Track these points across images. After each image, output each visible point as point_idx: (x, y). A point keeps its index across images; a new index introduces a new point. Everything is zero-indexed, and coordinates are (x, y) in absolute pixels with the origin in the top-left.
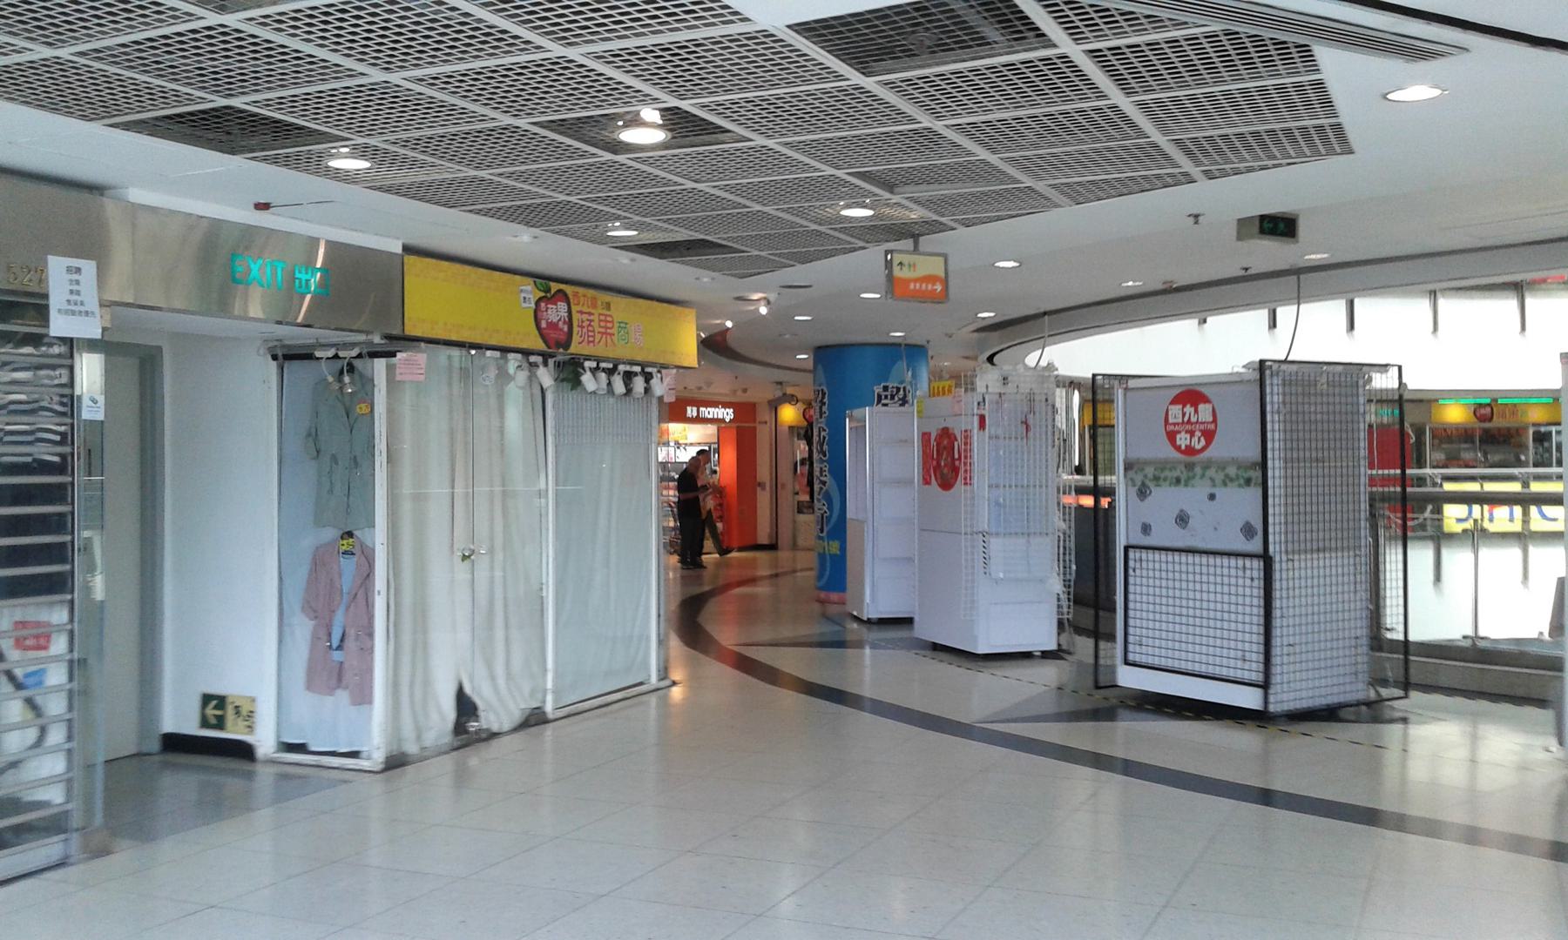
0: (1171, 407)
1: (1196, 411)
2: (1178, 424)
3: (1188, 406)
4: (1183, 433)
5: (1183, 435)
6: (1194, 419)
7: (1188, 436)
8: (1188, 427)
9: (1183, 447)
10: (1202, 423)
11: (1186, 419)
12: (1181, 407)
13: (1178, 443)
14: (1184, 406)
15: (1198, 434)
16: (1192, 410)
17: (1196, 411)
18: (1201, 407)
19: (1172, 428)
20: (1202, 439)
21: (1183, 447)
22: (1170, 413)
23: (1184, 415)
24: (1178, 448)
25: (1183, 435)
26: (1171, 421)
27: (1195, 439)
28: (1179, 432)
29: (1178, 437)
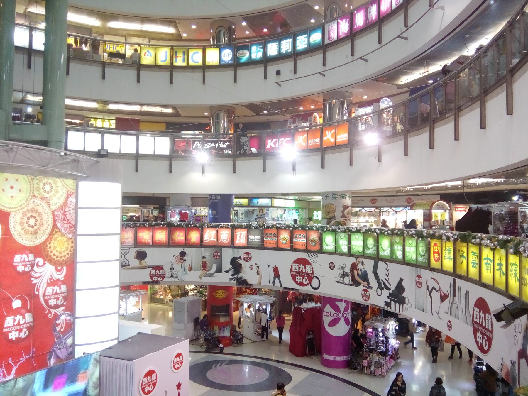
0: (293, 264)
1: (305, 268)
2: (297, 272)
3: (302, 265)
4: (299, 276)
5: (299, 277)
6: (304, 271)
7: (301, 278)
8: (301, 274)
9: (299, 282)
10: (308, 273)
11: (300, 270)
12: (298, 265)
13: (297, 280)
14: (300, 265)
15: (306, 278)
16: (303, 267)
17: (305, 268)
18: (307, 266)
19: (294, 273)
20: (307, 280)
21: (299, 282)
22: (293, 266)
23: (299, 268)
24: (297, 282)
25: (299, 277)
26: (293, 270)
27: (304, 280)
28: (297, 276)
29: (297, 277)
